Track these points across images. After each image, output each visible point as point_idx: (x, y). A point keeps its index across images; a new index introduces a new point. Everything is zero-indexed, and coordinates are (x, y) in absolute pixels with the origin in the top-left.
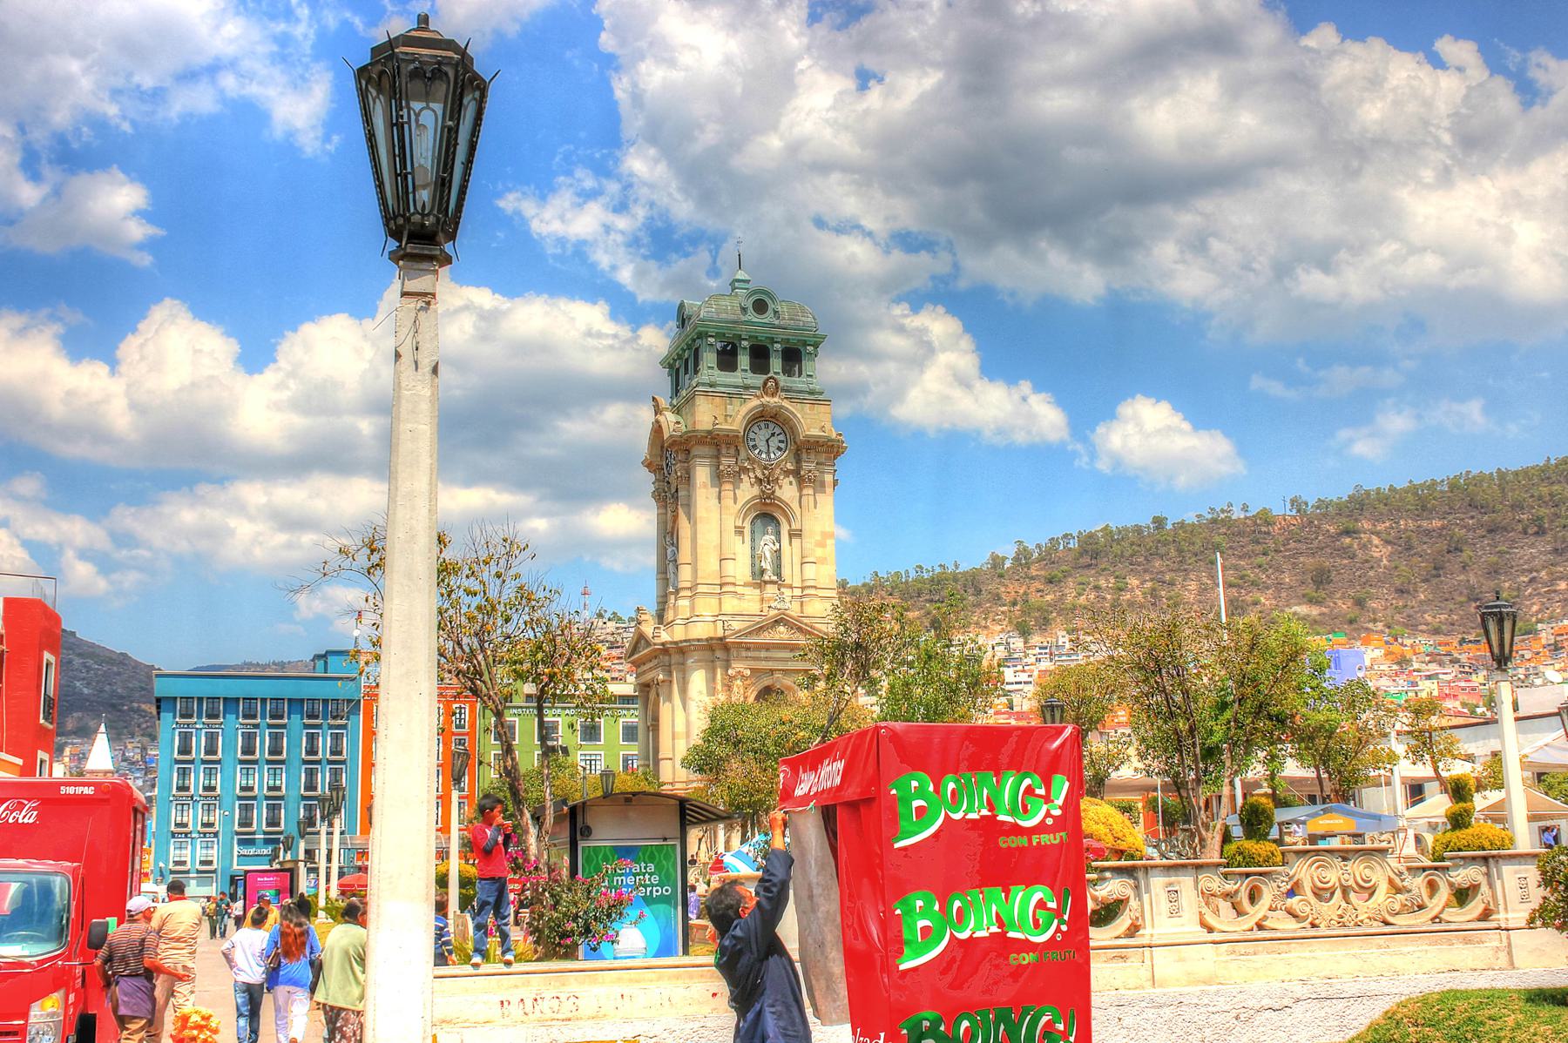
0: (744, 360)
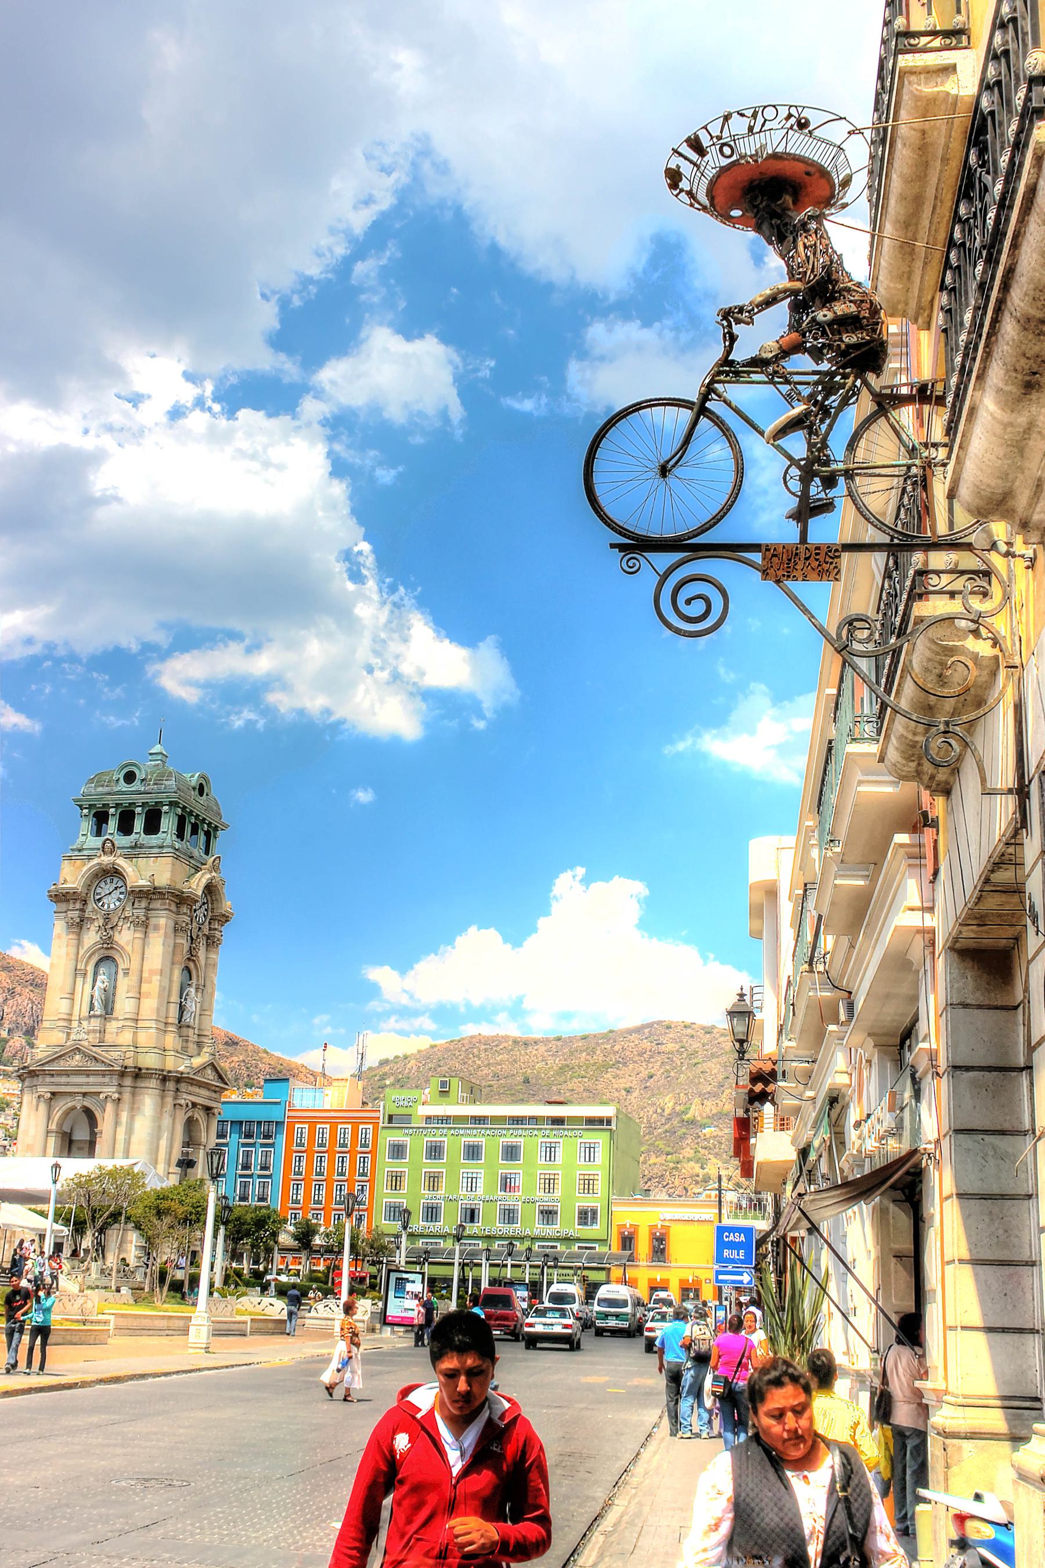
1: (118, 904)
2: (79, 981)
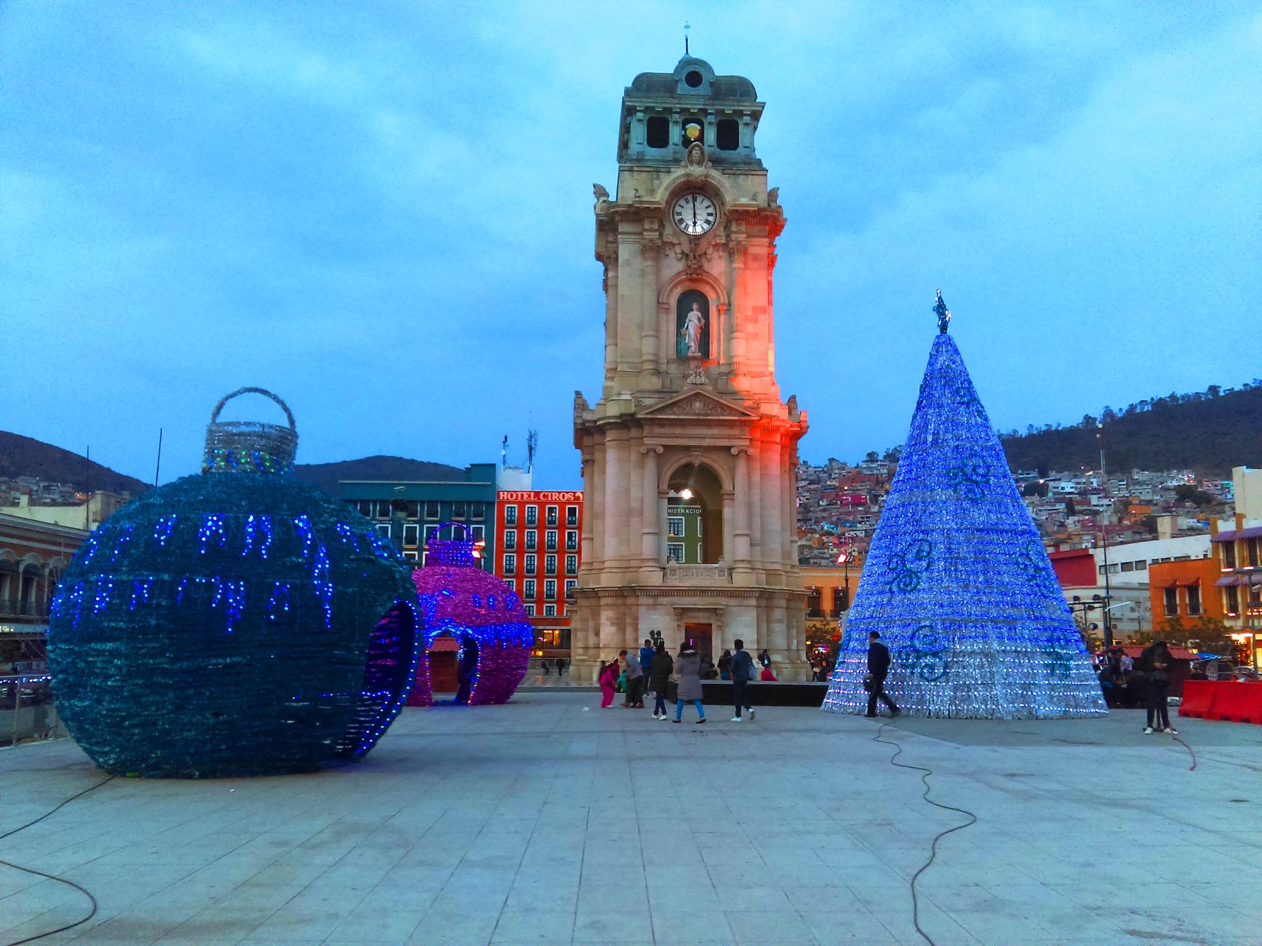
0: (675, 134)
1: (706, 226)
2: (663, 316)
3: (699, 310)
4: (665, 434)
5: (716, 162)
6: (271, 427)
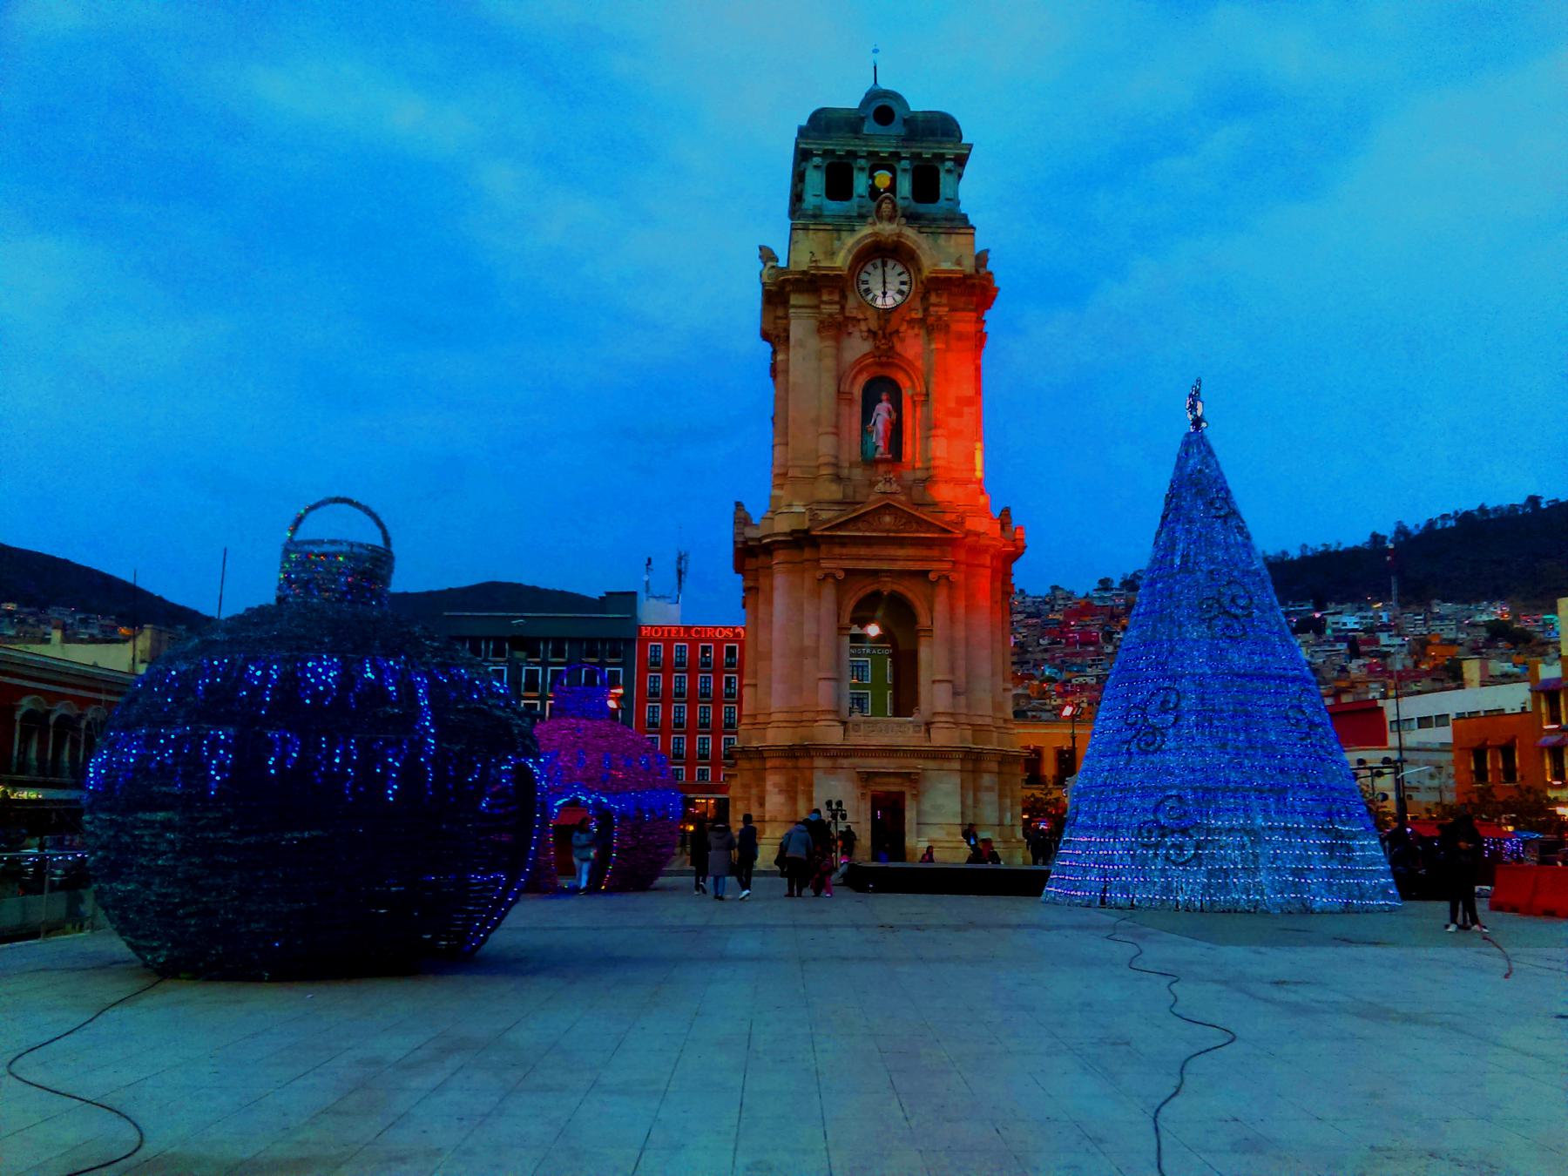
0: (861, 183)
1: (899, 298)
2: (845, 410)
3: (888, 400)
4: (847, 555)
5: (912, 218)
6: (361, 545)
